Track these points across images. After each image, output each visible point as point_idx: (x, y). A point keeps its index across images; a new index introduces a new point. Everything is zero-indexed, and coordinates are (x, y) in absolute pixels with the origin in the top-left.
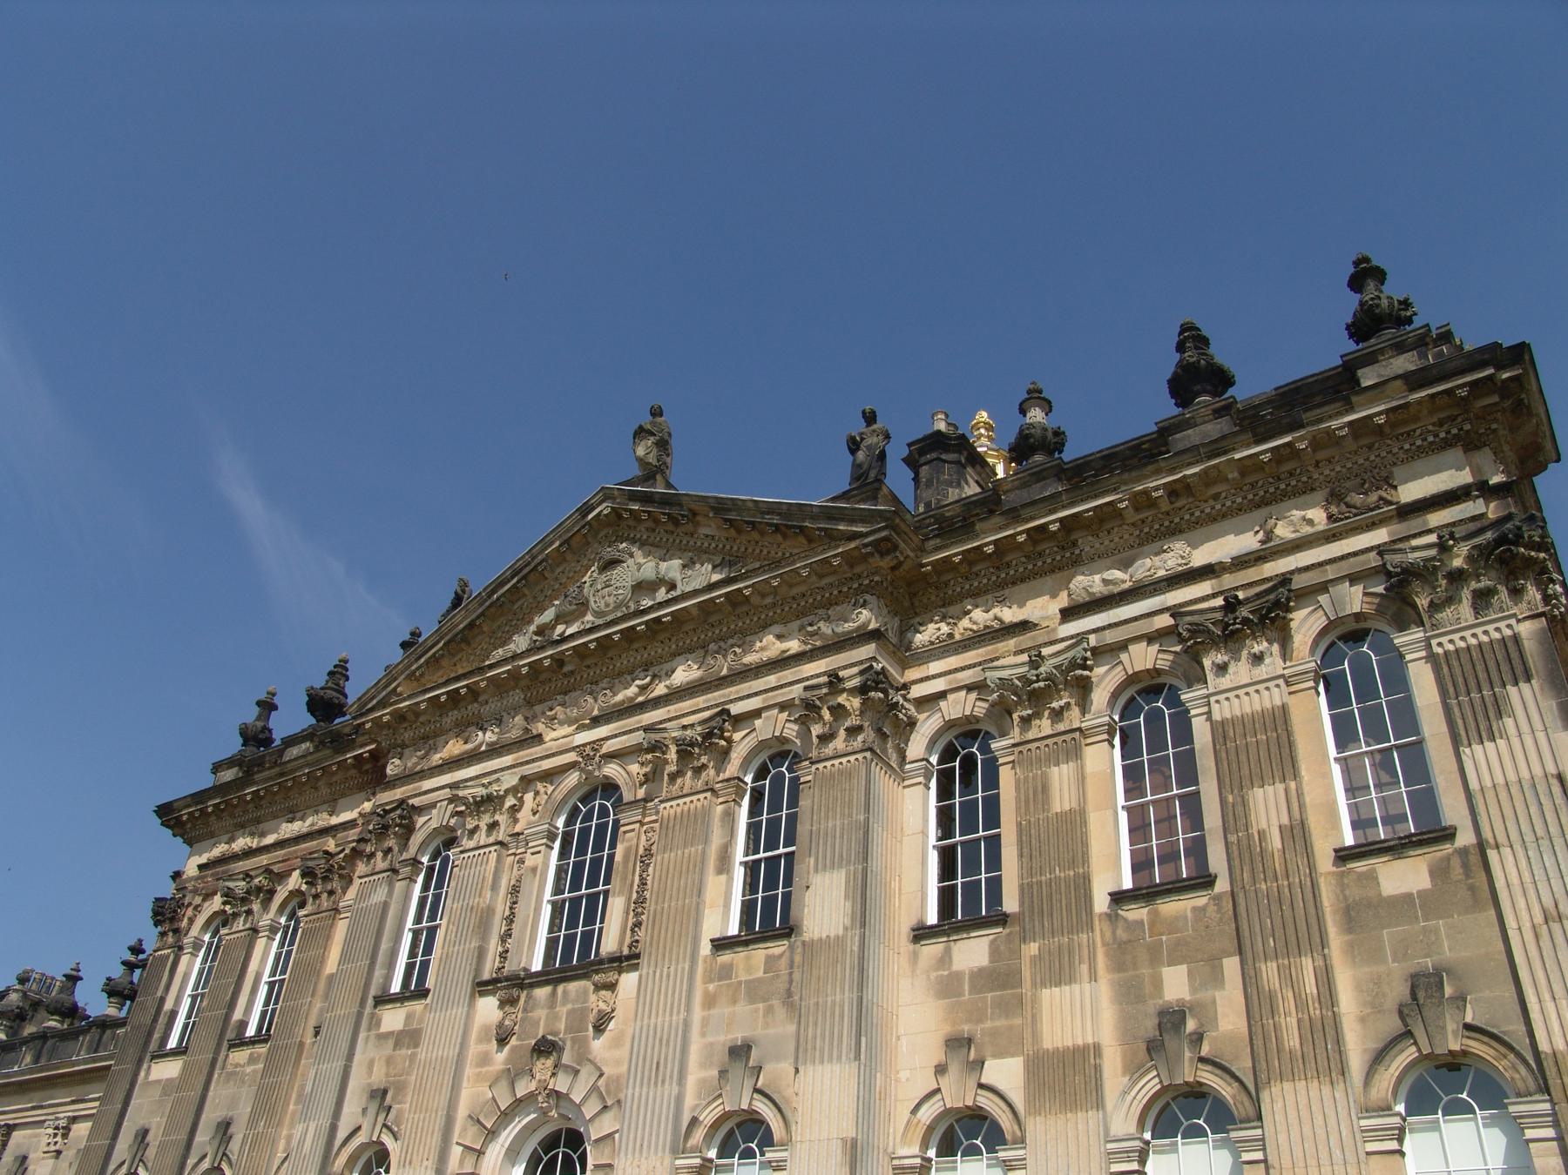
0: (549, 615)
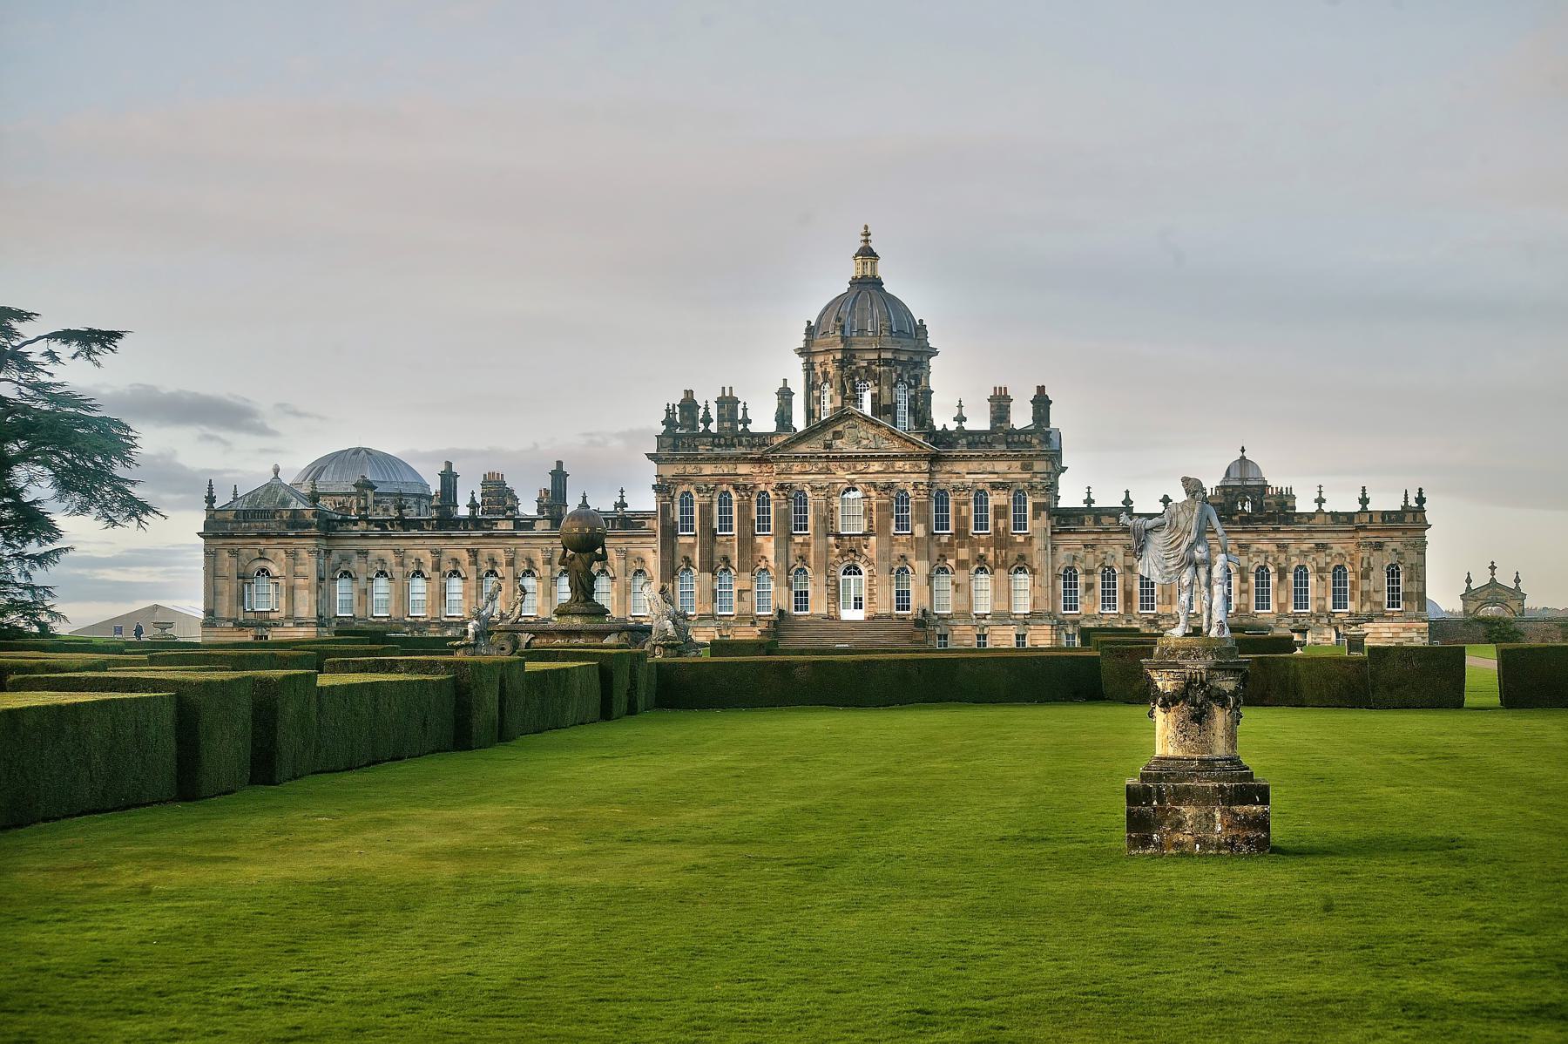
0: (829, 436)
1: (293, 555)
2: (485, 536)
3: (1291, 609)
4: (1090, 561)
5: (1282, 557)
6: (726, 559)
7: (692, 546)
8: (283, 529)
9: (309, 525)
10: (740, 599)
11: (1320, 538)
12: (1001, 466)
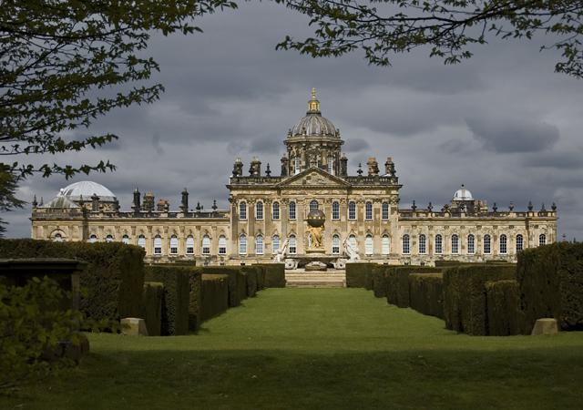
0: (305, 178)
1: (72, 228)
2: (155, 220)
3: (499, 253)
4: (416, 232)
5: (495, 231)
6: (260, 230)
7: (245, 225)
8: (68, 217)
9: (79, 215)
10: (266, 247)
11: (511, 223)
12: (378, 192)
